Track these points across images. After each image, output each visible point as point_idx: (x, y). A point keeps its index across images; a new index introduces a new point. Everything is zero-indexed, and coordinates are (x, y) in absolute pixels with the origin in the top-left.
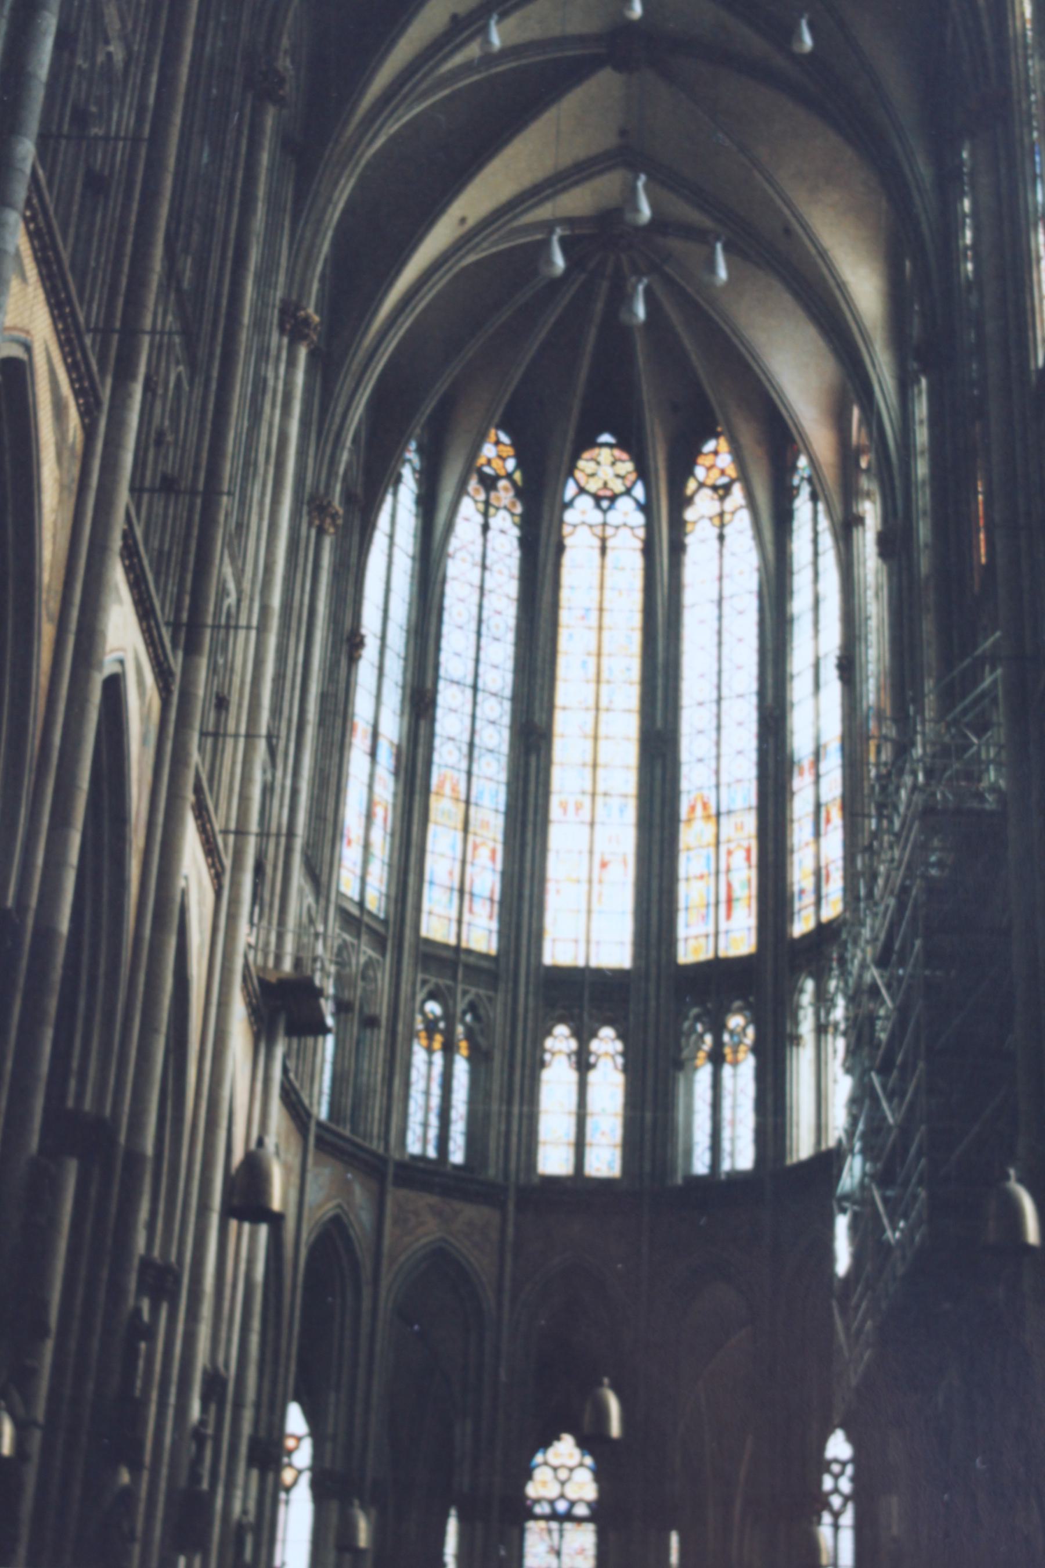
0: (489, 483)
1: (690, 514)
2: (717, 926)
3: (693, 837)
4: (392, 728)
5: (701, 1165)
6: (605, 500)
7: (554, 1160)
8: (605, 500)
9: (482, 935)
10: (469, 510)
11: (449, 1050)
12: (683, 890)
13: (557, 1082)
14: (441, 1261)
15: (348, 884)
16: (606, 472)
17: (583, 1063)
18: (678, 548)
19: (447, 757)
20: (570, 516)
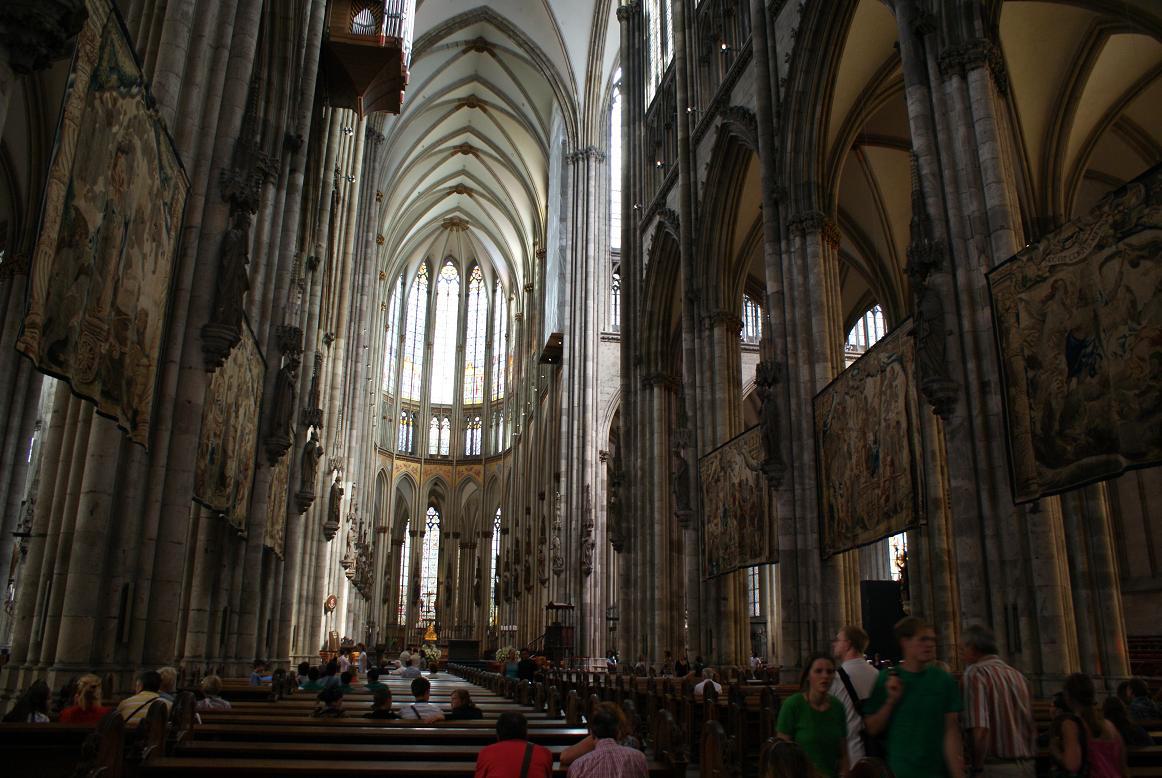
0: (420, 277)
1: (471, 286)
2: (473, 396)
3: (469, 372)
4: (395, 346)
5: (468, 453)
6: (448, 281)
7: (433, 451)
8: (448, 281)
9: (416, 397)
10: (415, 285)
11: (408, 425)
12: (465, 386)
13: (434, 433)
14: (407, 478)
15: (385, 388)
16: (450, 273)
17: (440, 428)
18: (467, 295)
19: (408, 350)
20: (439, 285)
